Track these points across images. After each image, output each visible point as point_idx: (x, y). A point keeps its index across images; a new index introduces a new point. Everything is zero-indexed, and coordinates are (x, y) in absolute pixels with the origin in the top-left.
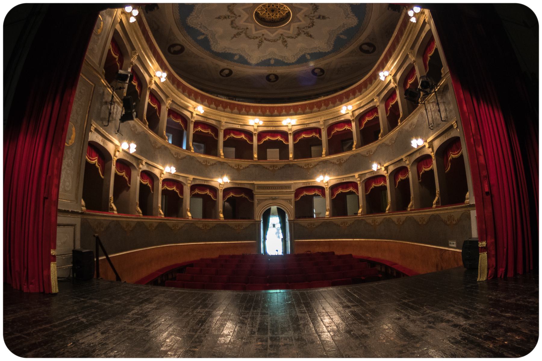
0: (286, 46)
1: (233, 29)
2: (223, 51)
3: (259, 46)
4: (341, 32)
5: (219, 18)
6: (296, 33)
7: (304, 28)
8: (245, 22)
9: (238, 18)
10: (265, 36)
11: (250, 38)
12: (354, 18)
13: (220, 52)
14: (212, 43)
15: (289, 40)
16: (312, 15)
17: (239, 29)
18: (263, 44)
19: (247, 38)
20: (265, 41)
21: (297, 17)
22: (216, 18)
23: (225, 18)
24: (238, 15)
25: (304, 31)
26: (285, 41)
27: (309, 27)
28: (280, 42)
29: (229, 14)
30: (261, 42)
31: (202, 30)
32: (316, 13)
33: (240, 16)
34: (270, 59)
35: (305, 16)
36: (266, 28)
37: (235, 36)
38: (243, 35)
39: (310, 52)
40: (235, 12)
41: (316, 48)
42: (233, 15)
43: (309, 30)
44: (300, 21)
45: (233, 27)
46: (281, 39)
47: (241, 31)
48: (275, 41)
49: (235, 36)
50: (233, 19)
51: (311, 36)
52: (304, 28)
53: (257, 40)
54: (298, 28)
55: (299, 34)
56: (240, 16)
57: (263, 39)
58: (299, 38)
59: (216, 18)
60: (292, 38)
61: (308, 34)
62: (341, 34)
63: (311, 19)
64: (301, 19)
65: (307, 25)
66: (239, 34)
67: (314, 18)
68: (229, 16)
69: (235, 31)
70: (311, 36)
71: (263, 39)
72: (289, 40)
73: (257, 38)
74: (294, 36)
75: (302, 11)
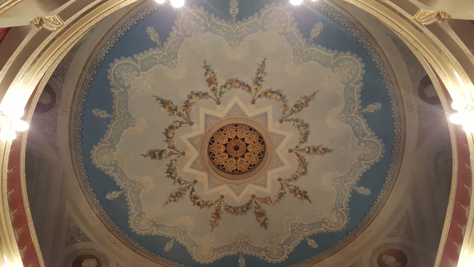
0: (207, 69)
1: (306, 122)
2: (342, 56)
3: (261, 69)
4: (111, 126)
5: (326, 150)
6: (193, 107)
7: (181, 123)
8: (283, 137)
9: (293, 148)
10: (250, 97)
11: (278, 93)
12: (103, 167)
13: (348, 55)
14: (358, 87)
15: (204, 88)
16: (173, 157)
17: (297, 121)
18: (255, 76)
19: (283, 93)
20: (251, 83)
21: (197, 149)
22: (330, 151)
23: (314, 150)
24: (293, 153)
25: (179, 115)
26: (210, 82)
27: (171, 127)
28: (221, 81)
29: (307, 157)
30: (258, 81)
31: (364, 126)
32: (169, 162)
33: (290, 151)
34: (240, 18)
35: (183, 154)
36: (248, 120)
37: (307, 100)
38: (291, 105)
39: (152, 52)
40: (297, 158)
41: (145, 69)
42: (301, 154)
43: (171, 120)
44: (191, 140)
45: (307, 125)
46: (218, 88)
47: (294, 116)
48: (231, 82)
49: (307, 100)
50: (303, 146)
51: (164, 103)
52: (181, 123)
53: (265, 87)
54: (191, 124)
55: (187, 105)
56: (290, 151)
57: (253, 87)
58: (183, 96)
59: (330, 151)
60: (197, 95)
61: (170, 109)
62: (108, 121)
63: (174, 148)
64: (189, 144)
65: (176, 131)
66: (299, 107)
67: (168, 150)
68: (308, 152)
69: (304, 115)
70: (164, 103)
71: (253, 87)
72: (204, 88)
73: (265, 94)
74: (195, 99)
75: (190, 163)
